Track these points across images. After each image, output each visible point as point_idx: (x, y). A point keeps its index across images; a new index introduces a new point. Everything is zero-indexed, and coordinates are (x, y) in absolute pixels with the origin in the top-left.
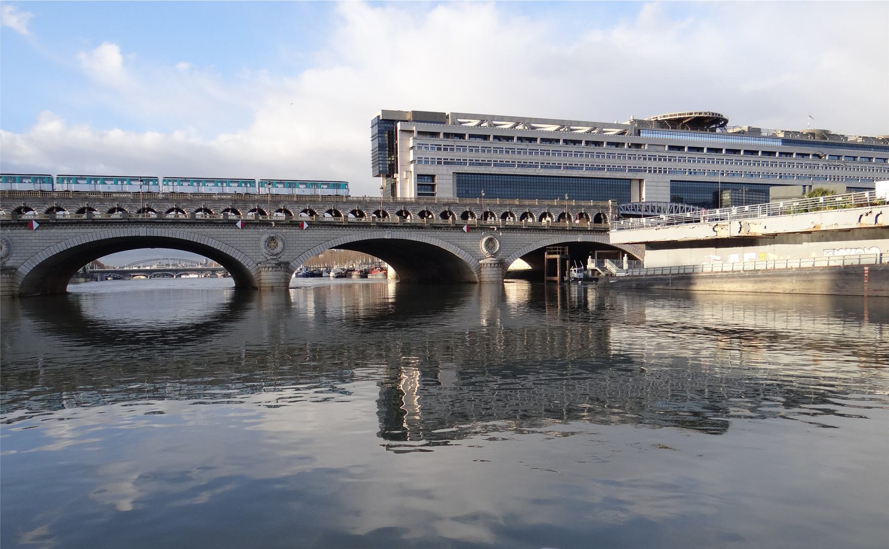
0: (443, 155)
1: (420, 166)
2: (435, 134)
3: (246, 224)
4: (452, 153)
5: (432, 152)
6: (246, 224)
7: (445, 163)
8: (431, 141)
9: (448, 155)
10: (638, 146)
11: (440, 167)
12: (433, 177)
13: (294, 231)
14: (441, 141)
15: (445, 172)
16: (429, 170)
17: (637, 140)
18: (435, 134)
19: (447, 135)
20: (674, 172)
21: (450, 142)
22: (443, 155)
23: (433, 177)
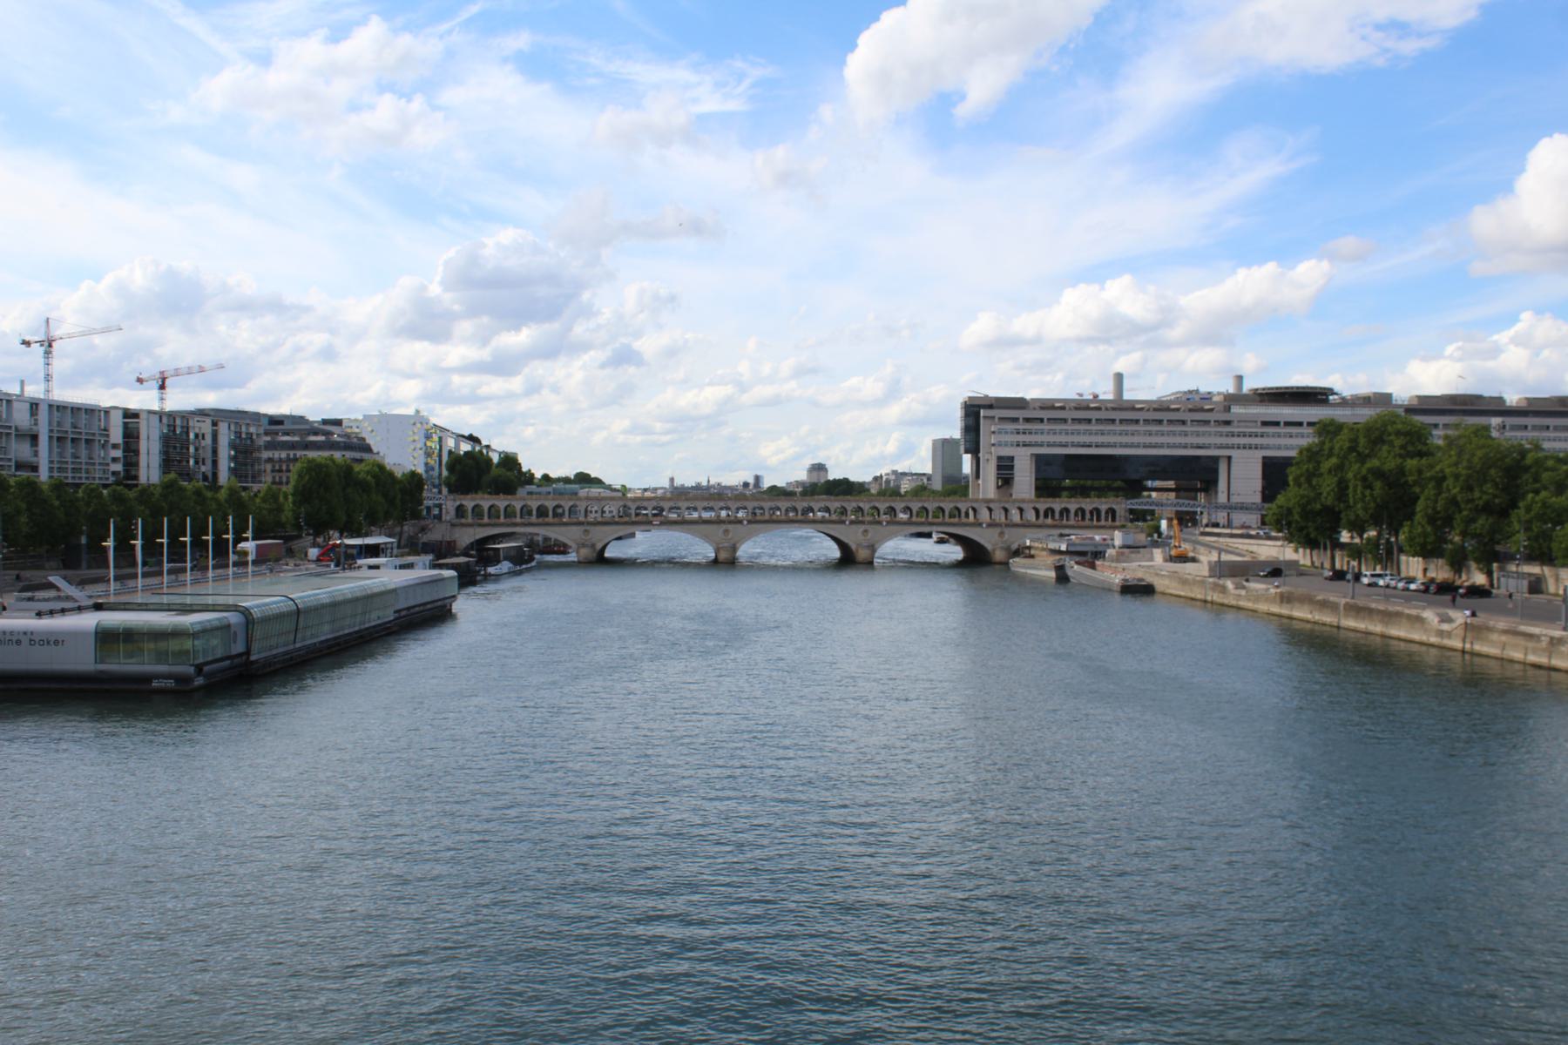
0: (1021, 438)
2: (1015, 420)
3: (852, 522)
6: (852, 522)
9: (1027, 438)
10: (1228, 423)
12: (1012, 459)
13: (877, 527)
14: (1021, 426)
16: (1006, 452)
17: (1225, 417)
18: (1015, 420)
19: (1027, 420)
20: (1267, 447)
21: (1028, 426)
22: (1021, 438)
23: (1012, 459)
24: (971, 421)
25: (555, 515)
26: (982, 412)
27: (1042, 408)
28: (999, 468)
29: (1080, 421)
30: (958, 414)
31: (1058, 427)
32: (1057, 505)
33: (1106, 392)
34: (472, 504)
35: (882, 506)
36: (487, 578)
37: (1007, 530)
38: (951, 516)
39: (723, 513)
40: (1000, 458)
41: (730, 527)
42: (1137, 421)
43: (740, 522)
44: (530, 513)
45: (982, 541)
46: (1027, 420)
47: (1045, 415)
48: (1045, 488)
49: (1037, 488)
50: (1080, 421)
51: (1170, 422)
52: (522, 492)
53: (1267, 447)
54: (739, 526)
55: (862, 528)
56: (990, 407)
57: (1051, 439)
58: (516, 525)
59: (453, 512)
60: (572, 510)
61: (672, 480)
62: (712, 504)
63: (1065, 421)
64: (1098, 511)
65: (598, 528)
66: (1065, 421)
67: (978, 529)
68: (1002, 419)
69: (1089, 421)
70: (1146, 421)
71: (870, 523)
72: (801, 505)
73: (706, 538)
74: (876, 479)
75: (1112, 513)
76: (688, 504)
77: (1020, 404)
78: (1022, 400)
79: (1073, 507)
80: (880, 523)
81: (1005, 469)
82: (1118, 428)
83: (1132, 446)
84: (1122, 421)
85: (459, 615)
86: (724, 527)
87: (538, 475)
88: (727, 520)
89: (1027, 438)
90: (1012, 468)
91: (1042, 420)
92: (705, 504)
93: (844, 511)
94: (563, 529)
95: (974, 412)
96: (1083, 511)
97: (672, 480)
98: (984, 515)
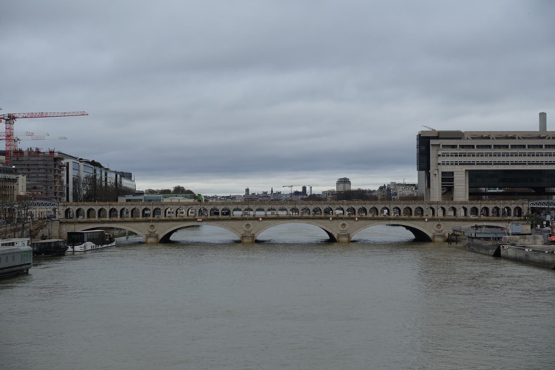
0: (458, 159)
1: (443, 166)
2: (454, 147)
4: (465, 158)
5: (452, 158)
7: (460, 164)
8: (450, 151)
9: (463, 159)
11: (457, 166)
12: (452, 173)
15: (460, 170)
18: (454, 147)
19: (462, 147)
21: (463, 151)
22: (458, 159)
23: (452, 173)
24: (423, 148)
25: (144, 215)
26: (432, 142)
27: (473, 138)
28: (443, 180)
29: (499, 147)
30: (414, 142)
31: (484, 151)
32: (480, 206)
33: (533, 126)
34: (77, 208)
35: (402, 207)
36: (74, 256)
37: (441, 223)
38: (504, 214)
39: (269, 213)
40: (444, 173)
41: (250, 222)
42: (541, 146)
43: (257, 219)
44: (217, 214)
45: (425, 231)
46: (462, 147)
47: (476, 143)
48: (474, 195)
49: (470, 194)
50: (499, 147)
51: (513, 147)
52: (122, 199)
53: (469, 164)
54: (256, 222)
55: (342, 222)
56: (437, 138)
57: (480, 159)
58: (104, 222)
59: (63, 215)
60: (156, 212)
61: (247, 190)
62: (239, 207)
63: (490, 147)
64: (486, 209)
65: (160, 224)
66: (490, 147)
67: (422, 223)
68: (444, 146)
69: (507, 147)
70: (548, 146)
71: (346, 219)
72: (323, 207)
73: (234, 229)
74: (381, 188)
75: (519, 211)
76: (279, 207)
77: (458, 135)
78: (459, 133)
79: (491, 207)
80: (353, 219)
81: (448, 180)
82: (527, 151)
83: (537, 163)
84: (529, 147)
85: (34, 277)
86: (246, 223)
87: (172, 189)
88: (246, 219)
89: (463, 159)
90: (452, 180)
91: (473, 147)
92: (258, 207)
93: (353, 210)
94: (137, 225)
95: (425, 142)
96: (498, 209)
97: (247, 190)
98: (428, 213)
